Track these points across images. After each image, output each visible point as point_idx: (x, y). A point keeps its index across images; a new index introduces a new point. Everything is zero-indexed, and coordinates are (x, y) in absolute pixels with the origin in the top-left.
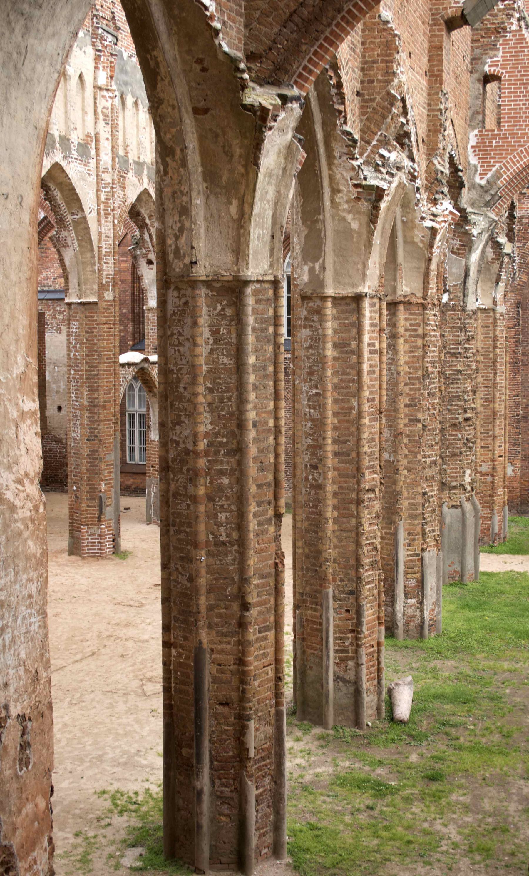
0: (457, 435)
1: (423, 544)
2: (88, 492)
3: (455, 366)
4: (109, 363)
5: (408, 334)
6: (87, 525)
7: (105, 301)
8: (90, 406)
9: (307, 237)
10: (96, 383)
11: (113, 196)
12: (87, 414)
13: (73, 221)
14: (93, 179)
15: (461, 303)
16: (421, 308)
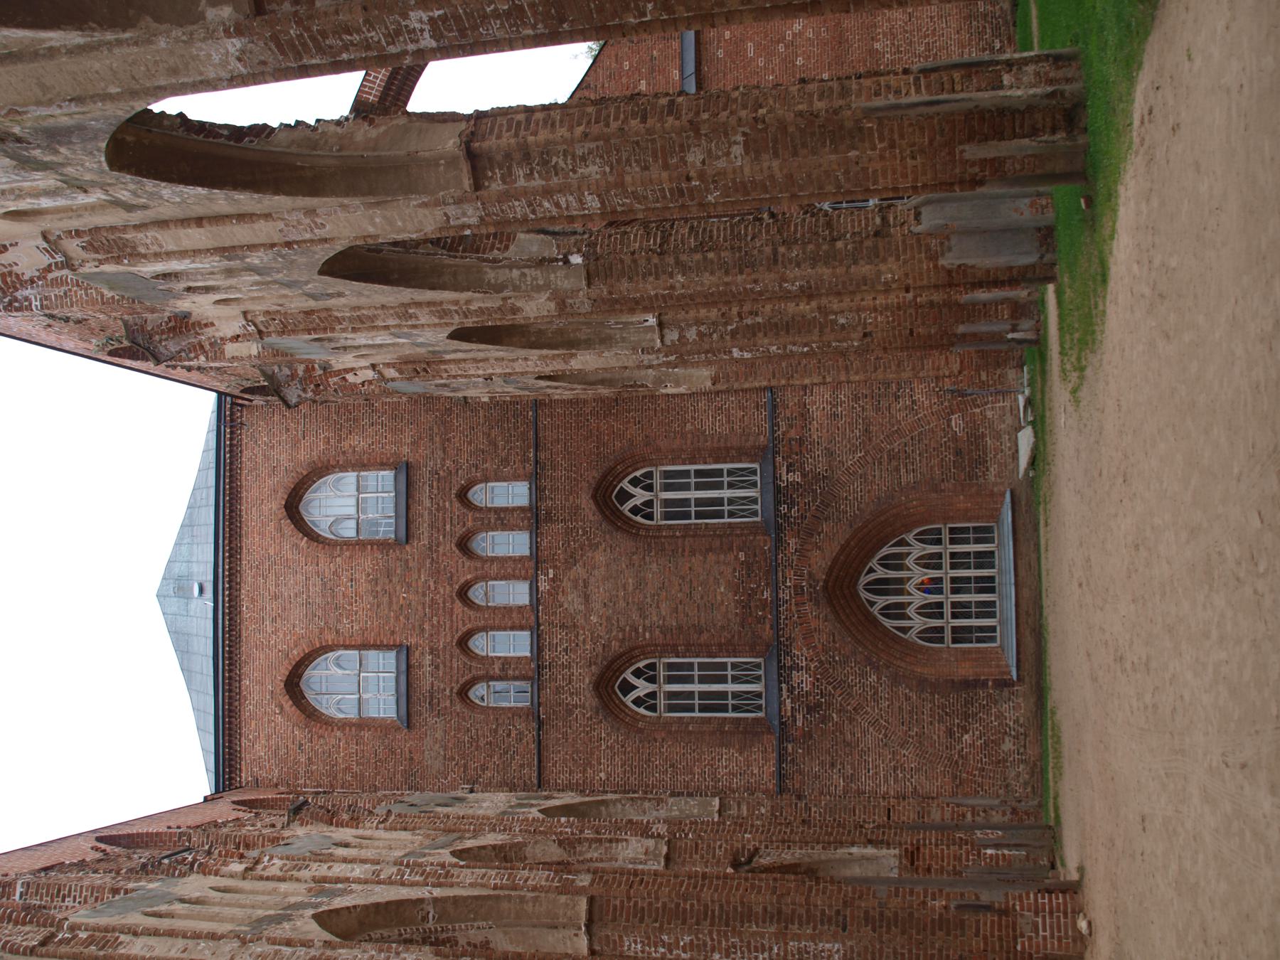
0: (796, 225)
1: (896, 74)
2: (948, 934)
3: (683, 235)
4: (703, 886)
5: (522, 133)
6: (1015, 939)
7: (592, 884)
8: (779, 921)
9: (158, 20)
10: (735, 908)
11: (420, 865)
12: (794, 928)
13: (439, 920)
14: (378, 888)
15: (586, 236)
16: (485, 121)
